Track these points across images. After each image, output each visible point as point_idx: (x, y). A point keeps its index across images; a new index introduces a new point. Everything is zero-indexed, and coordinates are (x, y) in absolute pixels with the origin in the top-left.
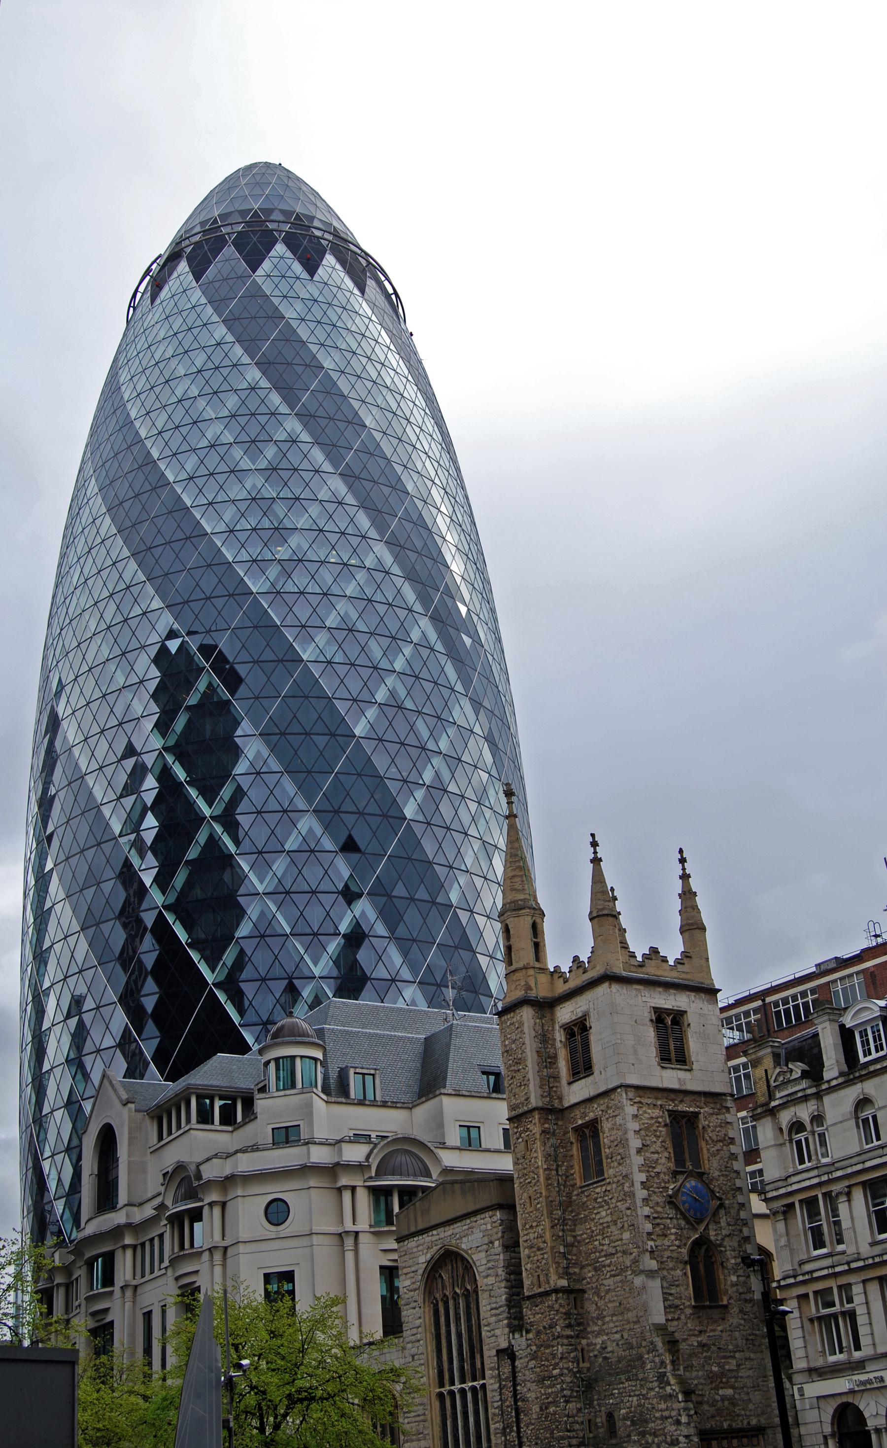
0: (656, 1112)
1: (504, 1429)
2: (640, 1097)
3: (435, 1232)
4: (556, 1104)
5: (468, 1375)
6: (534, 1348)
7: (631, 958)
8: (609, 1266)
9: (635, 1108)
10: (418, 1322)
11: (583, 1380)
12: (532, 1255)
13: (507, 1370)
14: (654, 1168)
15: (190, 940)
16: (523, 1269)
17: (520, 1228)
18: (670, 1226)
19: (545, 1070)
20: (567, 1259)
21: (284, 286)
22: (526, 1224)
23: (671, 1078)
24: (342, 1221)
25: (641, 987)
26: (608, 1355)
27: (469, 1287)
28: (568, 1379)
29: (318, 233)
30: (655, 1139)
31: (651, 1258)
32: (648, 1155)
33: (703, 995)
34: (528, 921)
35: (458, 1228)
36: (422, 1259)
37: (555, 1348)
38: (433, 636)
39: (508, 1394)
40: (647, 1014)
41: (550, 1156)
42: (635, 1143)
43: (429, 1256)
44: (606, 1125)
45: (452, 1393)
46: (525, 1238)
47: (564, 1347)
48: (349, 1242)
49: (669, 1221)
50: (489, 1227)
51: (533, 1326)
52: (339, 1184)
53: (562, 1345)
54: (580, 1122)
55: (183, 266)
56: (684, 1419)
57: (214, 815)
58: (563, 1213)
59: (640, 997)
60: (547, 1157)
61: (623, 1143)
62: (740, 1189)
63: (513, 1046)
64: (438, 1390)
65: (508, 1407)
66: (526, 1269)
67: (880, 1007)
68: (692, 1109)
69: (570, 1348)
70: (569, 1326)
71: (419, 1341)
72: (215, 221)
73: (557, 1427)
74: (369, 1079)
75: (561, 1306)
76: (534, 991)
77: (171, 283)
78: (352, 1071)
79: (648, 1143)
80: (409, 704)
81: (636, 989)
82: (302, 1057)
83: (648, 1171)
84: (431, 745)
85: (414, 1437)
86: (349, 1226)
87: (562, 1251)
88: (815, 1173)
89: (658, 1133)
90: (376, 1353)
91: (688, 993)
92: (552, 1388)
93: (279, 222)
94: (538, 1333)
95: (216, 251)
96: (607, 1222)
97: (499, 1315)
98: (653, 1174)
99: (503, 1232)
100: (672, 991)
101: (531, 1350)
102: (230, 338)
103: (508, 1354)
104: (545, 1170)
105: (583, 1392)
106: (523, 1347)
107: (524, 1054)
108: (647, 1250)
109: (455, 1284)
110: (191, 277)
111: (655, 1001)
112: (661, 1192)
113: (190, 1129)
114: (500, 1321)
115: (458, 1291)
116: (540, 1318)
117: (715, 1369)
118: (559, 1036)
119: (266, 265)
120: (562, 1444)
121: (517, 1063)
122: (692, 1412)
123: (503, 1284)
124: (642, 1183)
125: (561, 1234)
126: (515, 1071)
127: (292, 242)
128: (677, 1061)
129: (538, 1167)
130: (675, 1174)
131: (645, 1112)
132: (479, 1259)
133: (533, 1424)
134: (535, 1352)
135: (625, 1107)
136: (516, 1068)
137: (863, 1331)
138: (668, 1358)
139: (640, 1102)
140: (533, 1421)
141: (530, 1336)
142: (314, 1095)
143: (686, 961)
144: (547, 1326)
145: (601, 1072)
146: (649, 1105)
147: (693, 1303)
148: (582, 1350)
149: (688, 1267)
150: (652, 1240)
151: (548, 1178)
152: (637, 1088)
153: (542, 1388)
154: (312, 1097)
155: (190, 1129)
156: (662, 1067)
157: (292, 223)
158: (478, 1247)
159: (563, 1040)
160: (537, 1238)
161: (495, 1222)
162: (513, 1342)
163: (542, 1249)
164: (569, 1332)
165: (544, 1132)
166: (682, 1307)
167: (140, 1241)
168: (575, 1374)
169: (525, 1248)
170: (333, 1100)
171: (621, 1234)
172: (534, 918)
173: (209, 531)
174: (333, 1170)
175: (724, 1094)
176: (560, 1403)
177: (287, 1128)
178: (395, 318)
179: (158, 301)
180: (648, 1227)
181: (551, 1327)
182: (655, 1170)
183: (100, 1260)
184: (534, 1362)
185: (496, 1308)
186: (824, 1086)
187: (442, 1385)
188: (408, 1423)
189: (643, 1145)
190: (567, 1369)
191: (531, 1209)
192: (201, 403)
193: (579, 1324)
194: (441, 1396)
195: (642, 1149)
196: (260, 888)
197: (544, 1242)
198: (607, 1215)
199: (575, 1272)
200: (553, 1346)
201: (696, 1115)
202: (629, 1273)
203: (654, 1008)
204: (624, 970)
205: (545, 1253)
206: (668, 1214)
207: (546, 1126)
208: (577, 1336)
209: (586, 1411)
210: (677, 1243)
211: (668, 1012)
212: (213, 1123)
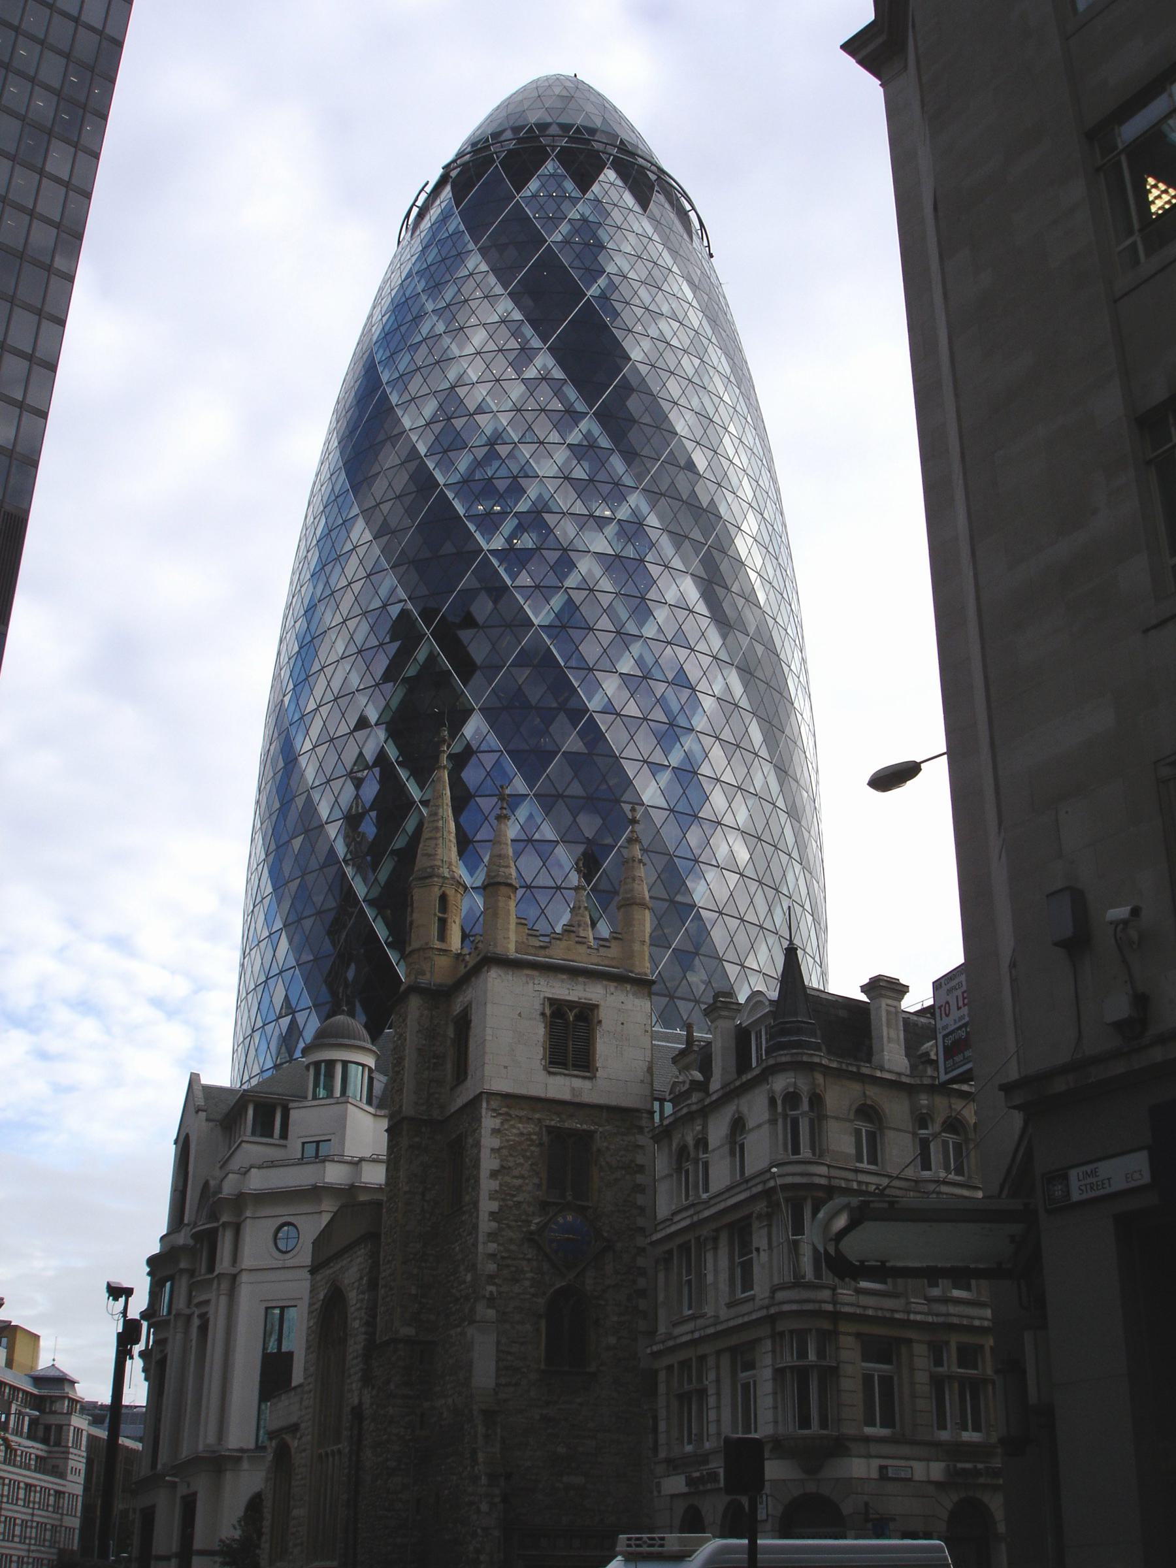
0: (530, 1128)
2: (508, 1107)
3: (332, 1264)
6: (374, 1407)
7: (530, 938)
9: (498, 1121)
14: (514, 1196)
15: (390, 939)
17: (381, 1263)
18: (525, 1269)
23: (561, 1087)
25: (536, 973)
29: (596, 145)
30: (522, 1161)
31: (489, 1307)
32: (507, 1179)
33: (629, 987)
34: (437, 892)
36: (322, 1297)
40: (538, 1007)
42: (488, 1163)
43: (326, 1291)
45: (327, 1454)
49: (525, 1263)
55: (447, 192)
56: (484, 1507)
57: (423, 799)
59: (531, 985)
61: (476, 1164)
62: (642, 1230)
63: (399, 1042)
67: (770, 1001)
68: (585, 1127)
72: (487, 140)
76: (428, 975)
77: (432, 212)
79: (511, 1164)
81: (527, 975)
82: (345, 1064)
83: (503, 1200)
87: (414, 1291)
88: (691, 1212)
89: (528, 1154)
91: (604, 982)
93: (553, 136)
98: (510, 1203)
100: (581, 979)
102: (484, 267)
103: (358, 1413)
104: (406, 1193)
108: (484, 1297)
111: (553, 991)
112: (519, 1226)
113: (242, 1141)
117: (561, 1450)
118: (451, 1033)
119: (533, 185)
122: (497, 1500)
123: (363, 1330)
124: (492, 1214)
125: (415, 1271)
127: (566, 158)
128: (574, 1065)
130: (544, 1206)
131: (513, 1127)
132: (352, 1296)
135: (483, 1120)
137: (712, 1415)
138: (481, 1429)
139: (507, 1114)
142: (349, 1105)
143: (614, 944)
146: (520, 1118)
147: (543, 1367)
149: (543, 1324)
150: (494, 1284)
152: (506, 1097)
154: (346, 1110)
155: (242, 1141)
156: (550, 1073)
157: (569, 137)
159: (452, 1036)
166: (525, 1370)
171: (466, 1275)
172: (443, 889)
175: (637, 1110)
177: (318, 1142)
178: (685, 236)
179: (418, 232)
180: (491, 1267)
182: (515, 1199)
183: (168, 1284)
185: (357, 1358)
186: (707, 1101)
189: (503, 1167)
192: (446, 340)
195: (498, 1171)
196: (467, 880)
201: (590, 1135)
202: (466, 1323)
203: (549, 999)
204: (516, 952)
206: (525, 1255)
207: (417, 1139)
210: (532, 1290)
211: (571, 1005)
212: (271, 1136)
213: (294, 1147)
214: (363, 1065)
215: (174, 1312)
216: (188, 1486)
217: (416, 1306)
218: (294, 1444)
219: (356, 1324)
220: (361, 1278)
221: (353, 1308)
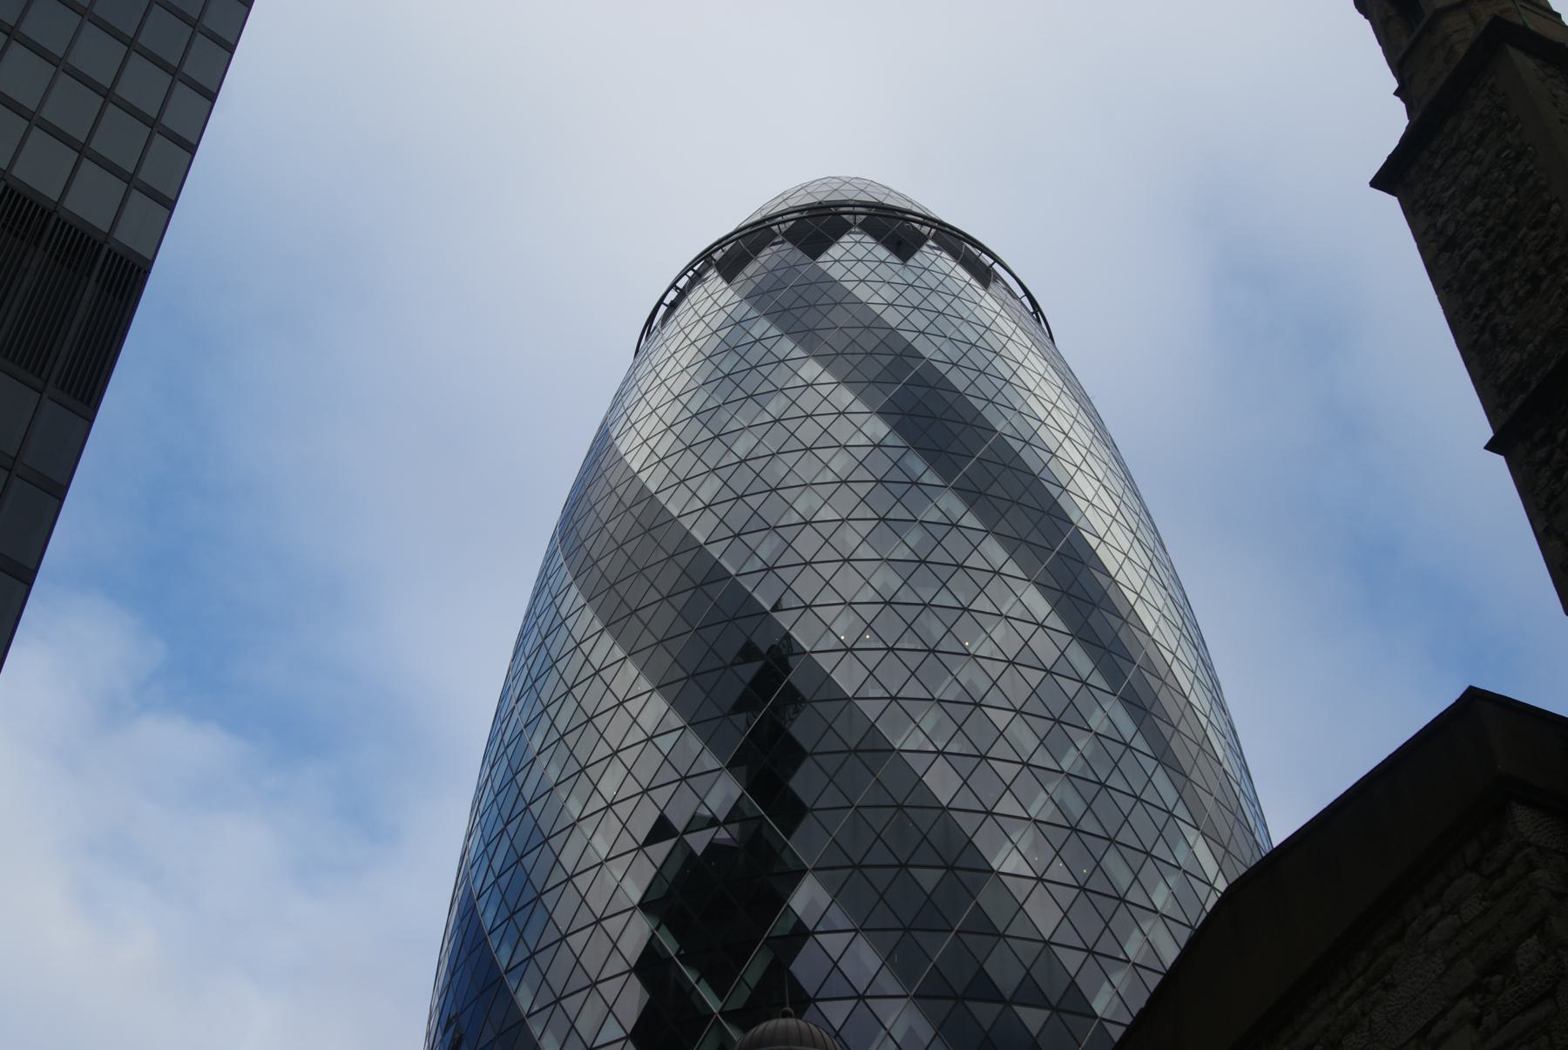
21: (861, 271)
38: (1127, 727)
57: (725, 1009)
80: (1089, 825)
84: (1135, 896)
95: (757, 249)
110: (720, 280)
119: (835, 251)
173: (733, 572)
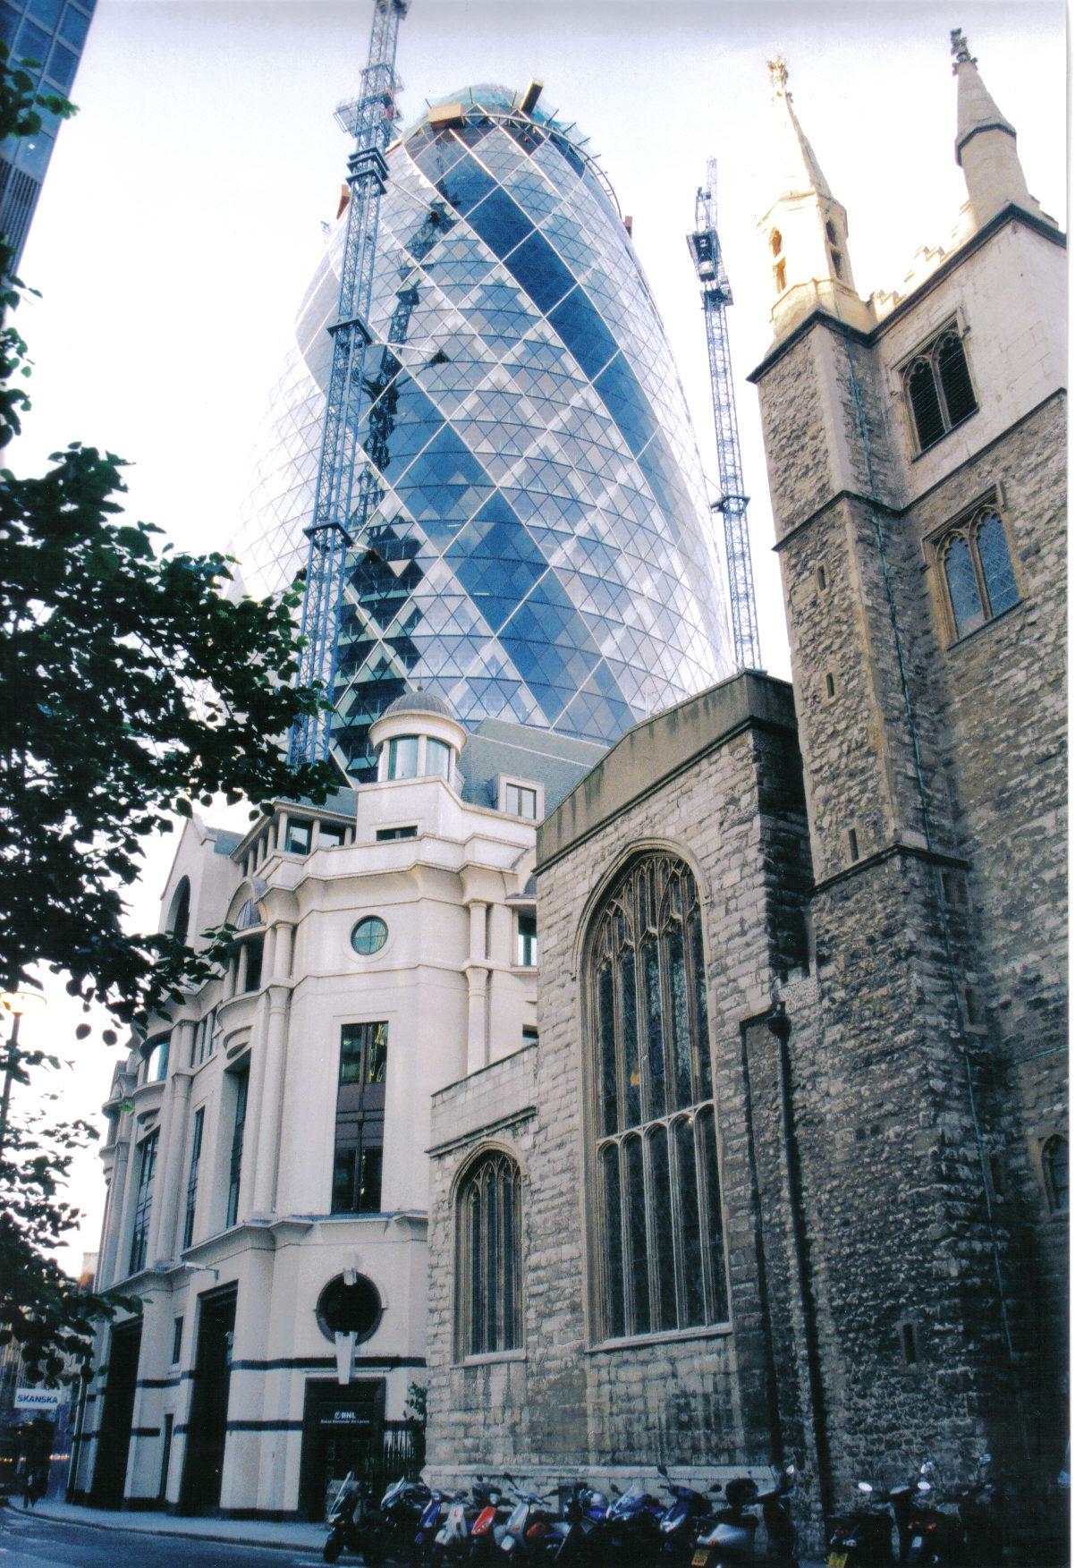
1: (756, 1196)
3: (610, 829)
4: (886, 501)
5: (671, 1096)
8: (1040, 786)
10: (567, 1011)
11: (974, 1063)
12: (835, 793)
13: (767, 1061)
16: (812, 829)
19: (861, 440)
20: (922, 793)
22: (818, 733)
24: (467, 955)
26: (1045, 995)
27: (678, 916)
28: (939, 1053)
35: (656, 804)
36: (583, 888)
37: (902, 981)
39: (770, 1116)
41: (877, 586)
43: (596, 877)
44: (1018, 493)
46: (816, 765)
47: (926, 979)
48: (477, 981)
50: (728, 772)
51: (837, 946)
52: (466, 900)
53: (921, 973)
54: (945, 519)
58: (912, 700)
60: (872, 588)
63: (791, 412)
64: (602, 1141)
65: (765, 1145)
66: (820, 829)
69: (940, 982)
70: (934, 933)
71: (568, 1045)
73: (909, 1174)
74: (527, 796)
75: (912, 883)
78: (503, 780)
82: (430, 739)
85: (551, 1240)
86: (477, 956)
87: (911, 773)
90: (489, 1086)
92: (892, 1077)
94: (854, 956)
96: (1032, 692)
97: (748, 945)
99: (760, 775)
101: (833, 1001)
105: (975, 1090)
106: (809, 1000)
107: (813, 414)
109: (648, 918)
114: (748, 958)
115: (653, 930)
116: (857, 922)
120: (924, 1214)
121: (798, 437)
126: (793, 454)
129: (851, 605)
133: (834, 1177)
134: (843, 1003)
136: (796, 447)
140: (835, 1170)
141: (829, 970)
144: (877, 936)
145: (999, 398)
148: (969, 993)
151: (874, 625)
153: (862, 1084)
158: (701, 822)
160: (849, 752)
161: (741, 759)
162: (784, 995)
163: (863, 771)
164: (934, 947)
165: (861, 540)
167: (202, 1016)
168: (954, 1042)
169: (816, 785)
170: (469, 806)
172: (829, 214)
174: (457, 878)
176: (920, 1110)
181: (887, 934)
184: (840, 1027)
187: (611, 1128)
188: (540, 1212)
190: (935, 1028)
191: (833, 699)
193: (959, 935)
194: (609, 1150)
197: (869, 754)
198: (1028, 678)
199: (941, 827)
200: (893, 979)
205: (871, 777)
208: (953, 961)
209: (985, 1137)
213: (366, 832)
214: (448, 746)
215: (171, 1071)
216: (217, 1278)
217: (919, 798)
218: (517, 1146)
219: (732, 877)
220: (734, 801)
221: (710, 861)
